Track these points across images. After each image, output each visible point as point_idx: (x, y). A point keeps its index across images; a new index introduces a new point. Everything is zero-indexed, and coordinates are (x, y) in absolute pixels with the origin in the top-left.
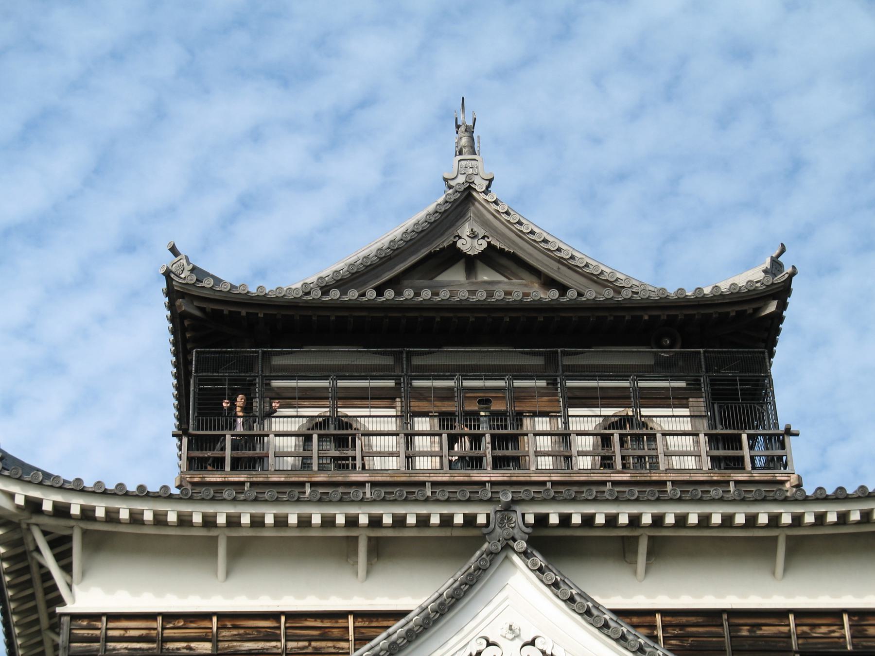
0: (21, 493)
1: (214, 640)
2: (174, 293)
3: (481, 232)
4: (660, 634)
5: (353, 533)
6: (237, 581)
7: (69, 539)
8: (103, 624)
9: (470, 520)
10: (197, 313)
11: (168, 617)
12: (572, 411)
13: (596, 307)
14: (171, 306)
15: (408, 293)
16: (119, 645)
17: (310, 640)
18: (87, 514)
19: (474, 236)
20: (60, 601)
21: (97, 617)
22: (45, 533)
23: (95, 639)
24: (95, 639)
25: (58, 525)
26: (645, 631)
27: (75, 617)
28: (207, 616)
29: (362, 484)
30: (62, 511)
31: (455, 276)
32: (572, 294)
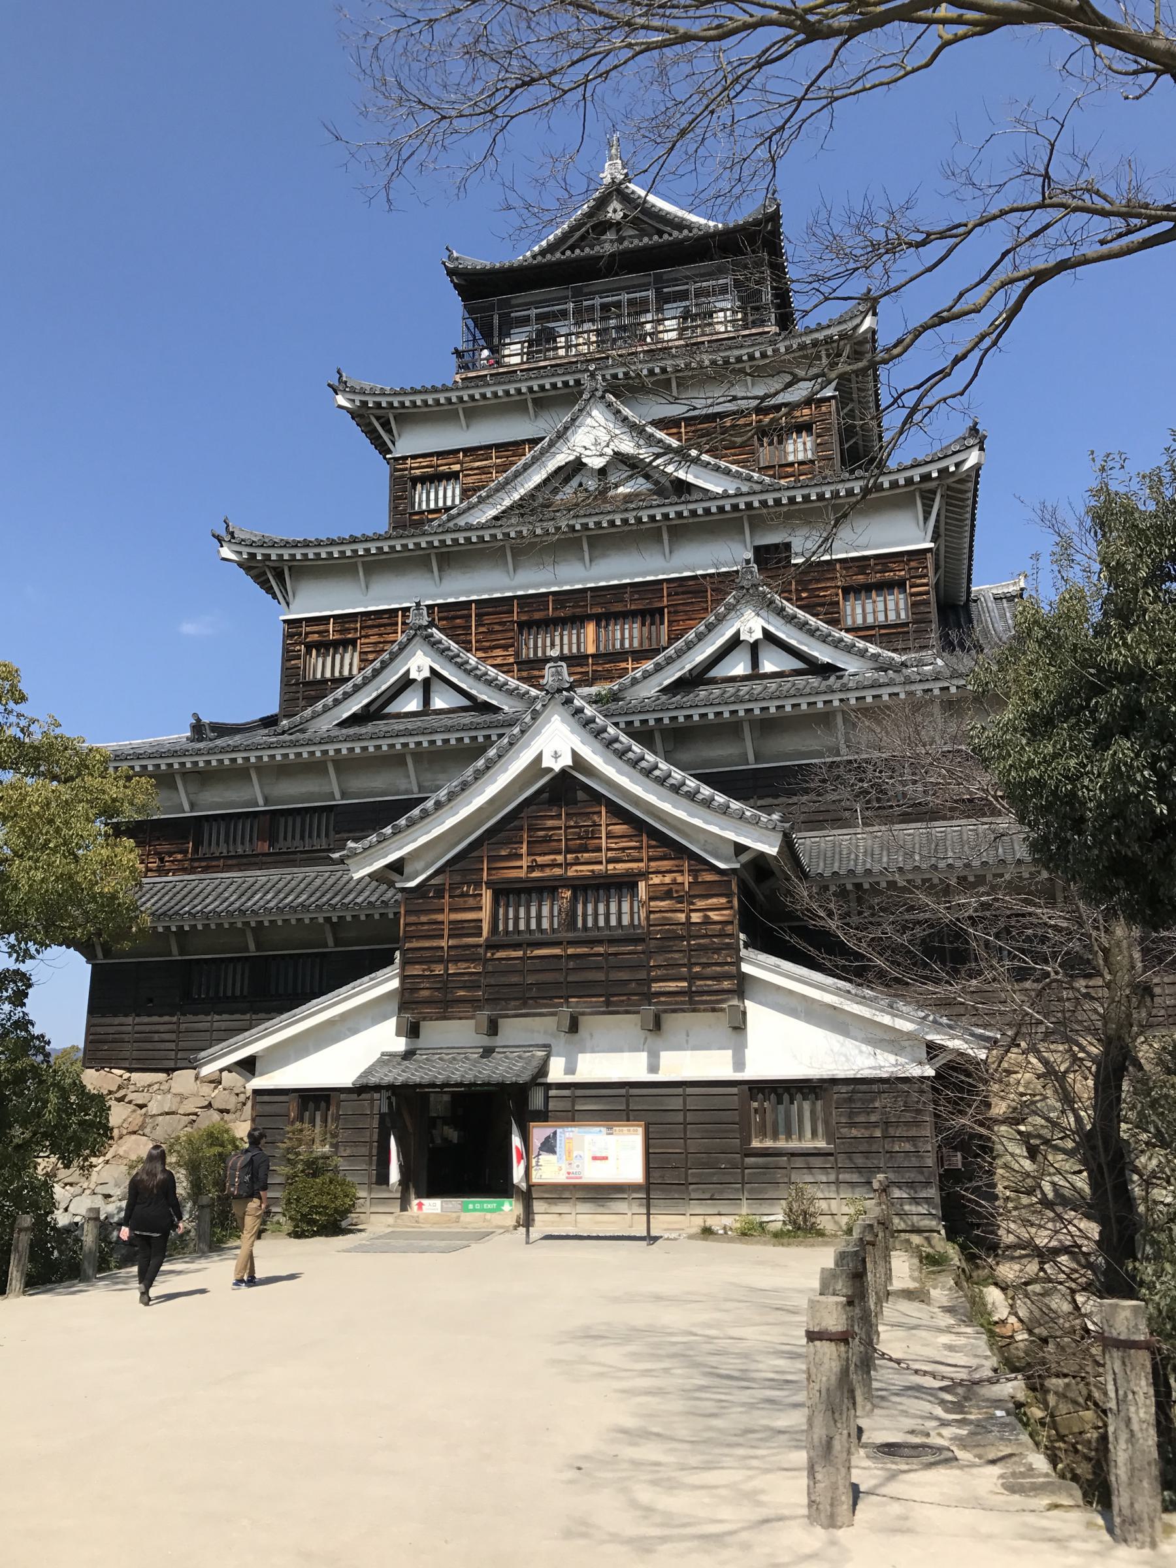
0: (358, 399)
1: (461, 463)
2: (451, 272)
3: (619, 207)
4: (683, 430)
5: (523, 397)
6: (473, 429)
7: (388, 422)
8: (409, 461)
9: (578, 382)
10: (463, 282)
11: (439, 454)
12: (666, 306)
13: (678, 243)
14: (452, 281)
15: (587, 250)
16: (417, 471)
17: (507, 457)
18: (390, 404)
19: (615, 211)
20: (390, 452)
21: (405, 458)
22: (378, 418)
23: (405, 469)
24: (405, 469)
25: (379, 412)
26: (674, 430)
27: (396, 459)
28: (457, 451)
29: (545, 367)
30: (378, 405)
31: (610, 235)
32: (666, 236)
